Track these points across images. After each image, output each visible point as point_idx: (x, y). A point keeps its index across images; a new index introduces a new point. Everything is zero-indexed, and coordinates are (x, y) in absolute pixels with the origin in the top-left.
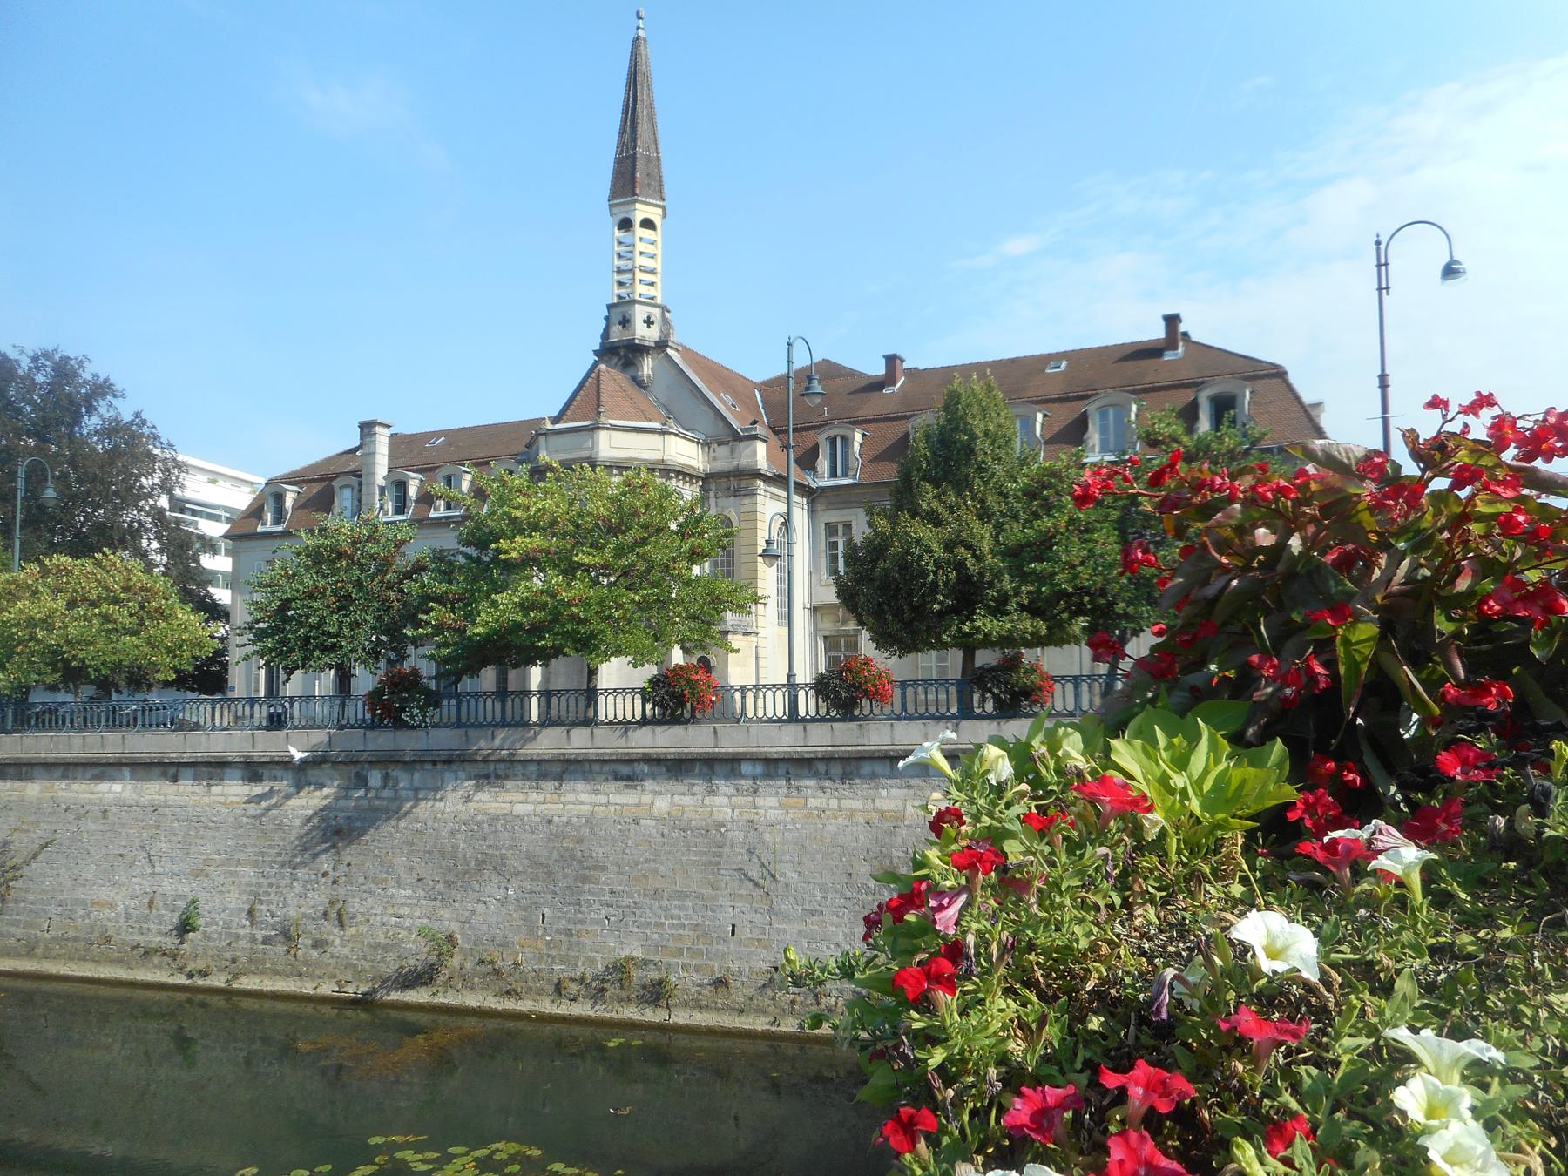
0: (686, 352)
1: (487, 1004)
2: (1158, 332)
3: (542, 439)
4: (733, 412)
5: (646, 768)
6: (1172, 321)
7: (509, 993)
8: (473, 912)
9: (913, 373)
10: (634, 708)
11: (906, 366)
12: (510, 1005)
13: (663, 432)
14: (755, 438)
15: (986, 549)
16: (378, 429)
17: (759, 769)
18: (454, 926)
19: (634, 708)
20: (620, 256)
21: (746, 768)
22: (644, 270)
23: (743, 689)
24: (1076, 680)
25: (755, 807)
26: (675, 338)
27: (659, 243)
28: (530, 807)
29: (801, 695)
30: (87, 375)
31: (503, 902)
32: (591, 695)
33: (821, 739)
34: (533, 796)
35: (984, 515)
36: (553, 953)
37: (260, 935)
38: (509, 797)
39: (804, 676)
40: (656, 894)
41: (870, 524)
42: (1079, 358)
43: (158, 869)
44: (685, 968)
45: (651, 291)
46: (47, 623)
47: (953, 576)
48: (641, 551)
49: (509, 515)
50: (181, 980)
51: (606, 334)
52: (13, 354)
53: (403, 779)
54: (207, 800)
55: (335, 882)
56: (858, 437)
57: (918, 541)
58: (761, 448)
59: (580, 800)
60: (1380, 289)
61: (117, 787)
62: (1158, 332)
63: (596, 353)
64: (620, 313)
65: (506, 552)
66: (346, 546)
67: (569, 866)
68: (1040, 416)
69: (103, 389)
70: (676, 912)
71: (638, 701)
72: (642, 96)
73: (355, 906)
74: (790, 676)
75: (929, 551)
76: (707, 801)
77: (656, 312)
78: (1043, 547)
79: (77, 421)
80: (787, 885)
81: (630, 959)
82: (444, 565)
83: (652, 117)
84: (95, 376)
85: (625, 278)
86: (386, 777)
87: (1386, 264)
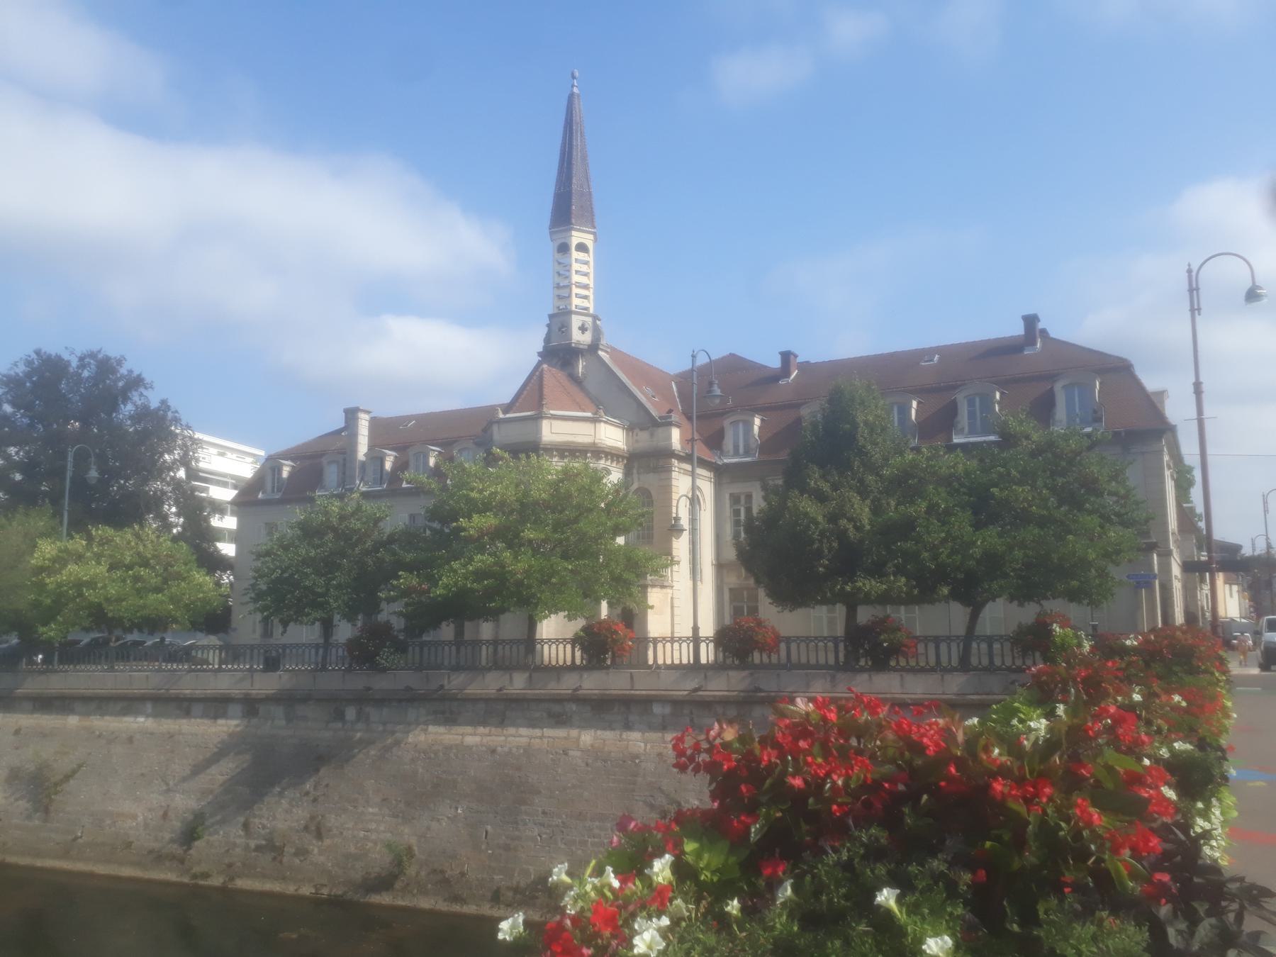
0: (614, 352)
1: (438, 907)
2: (1018, 329)
3: (495, 428)
5: (574, 707)
6: (1031, 321)
7: (456, 899)
8: (428, 828)
9: (806, 367)
11: (799, 360)
12: (456, 908)
13: (594, 420)
14: (670, 424)
16: (362, 415)
17: (667, 710)
18: (413, 841)
20: (559, 274)
21: (657, 709)
22: (579, 286)
23: (655, 641)
24: (937, 640)
26: (603, 342)
27: (592, 264)
28: (477, 739)
29: (703, 646)
30: (123, 371)
32: (530, 642)
33: (719, 687)
34: (481, 730)
35: (863, 492)
37: (253, 844)
38: (461, 729)
39: (708, 629)
41: (765, 498)
42: (948, 353)
45: (585, 303)
46: (91, 584)
47: (835, 545)
50: (186, 880)
51: (548, 339)
52: (66, 356)
54: (214, 730)
55: (315, 800)
56: (757, 421)
57: (806, 514)
58: (676, 434)
59: (518, 737)
60: (1192, 310)
61: (141, 719)
62: (1018, 329)
63: (540, 354)
64: (559, 321)
65: (464, 530)
66: (335, 521)
68: (914, 404)
69: (137, 382)
70: (596, 831)
71: (569, 647)
72: (577, 142)
73: (332, 821)
74: (696, 629)
75: (817, 524)
76: (624, 736)
78: (907, 527)
79: (114, 407)
82: (408, 538)
83: (584, 158)
84: (131, 372)
85: (564, 293)
87: (1197, 289)
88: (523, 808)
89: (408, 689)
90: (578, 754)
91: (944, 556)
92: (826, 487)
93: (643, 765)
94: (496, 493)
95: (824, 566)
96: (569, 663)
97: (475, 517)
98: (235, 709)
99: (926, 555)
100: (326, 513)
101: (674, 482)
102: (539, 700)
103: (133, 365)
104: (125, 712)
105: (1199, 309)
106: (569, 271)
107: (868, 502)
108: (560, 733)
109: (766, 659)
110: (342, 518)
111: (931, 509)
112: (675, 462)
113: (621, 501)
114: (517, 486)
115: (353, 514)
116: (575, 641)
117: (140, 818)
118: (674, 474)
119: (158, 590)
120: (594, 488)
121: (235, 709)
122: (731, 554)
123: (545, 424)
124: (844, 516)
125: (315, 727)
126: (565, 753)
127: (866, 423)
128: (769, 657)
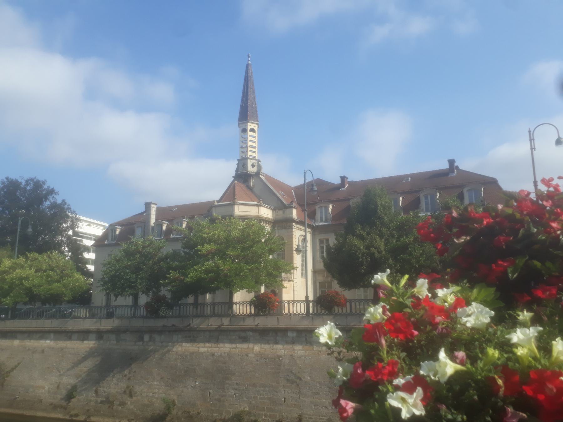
0: (267, 176)
2: (446, 166)
3: (213, 209)
4: (284, 198)
6: (451, 162)
8: (182, 391)
9: (352, 183)
10: (246, 310)
11: (349, 180)
13: (258, 206)
14: (292, 207)
15: (383, 249)
16: (153, 206)
17: (295, 334)
18: (175, 398)
19: (246, 310)
21: (290, 334)
22: (251, 147)
23: (289, 302)
25: (294, 350)
27: (257, 137)
28: (206, 349)
29: (311, 304)
30: (45, 187)
31: (194, 387)
32: (230, 304)
34: (207, 345)
35: (381, 236)
36: (213, 408)
40: (254, 385)
41: (336, 239)
42: (415, 177)
43: (62, 372)
44: (265, 416)
45: (254, 155)
46: (27, 278)
48: (251, 249)
49: (202, 236)
50: (67, 417)
51: (237, 170)
52: (20, 180)
53: (157, 337)
55: (129, 379)
56: (331, 207)
57: (356, 245)
58: (295, 212)
59: (225, 348)
60: (532, 149)
61: (48, 341)
62: (446, 166)
63: (234, 177)
64: (242, 162)
65: (200, 251)
66: (140, 249)
67: (220, 374)
68: (401, 198)
69: (51, 192)
70: (262, 392)
72: (250, 85)
73: (137, 389)
74: (307, 297)
76: (274, 347)
77: (256, 162)
78: (404, 248)
79: (41, 203)
80: (306, 382)
81: (243, 411)
82: (175, 255)
83: (253, 91)
84: (49, 187)
85: (244, 150)
86: (151, 338)
87: (533, 140)
88: (227, 381)
89: (173, 325)
90: (253, 356)
91: (422, 261)
92: (364, 233)
93: (283, 361)
94: (215, 234)
95: (364, 270)
96: (248, 312)
97: (205, 245)
98: (93, 336)
99: (414, 261)
100: (136, 245)
101: (294, 233)
102: (234, 331)
103: (50, 184)
104: (41, 338)
105: (535, 148)
106: (247, 140)
107: (383, 240)
108: (245, 346)
109: (340, 311)
110: (144, 247)
111: (415, 239)
112: (294, 224)
113: (272, 239)
114: (225, 231)
115: (149, 246)
116: (251, 303)
117: (47, 388)
118: (294, 230)
119: (58, 281)
120: (260, 232)
121: (93, 336)
122: (321, 266)
123: (236, 207)
124: (373, 246)
125: (130, 345)
126: (247, 355)
127: (381, 205)
128: (342, 309)
